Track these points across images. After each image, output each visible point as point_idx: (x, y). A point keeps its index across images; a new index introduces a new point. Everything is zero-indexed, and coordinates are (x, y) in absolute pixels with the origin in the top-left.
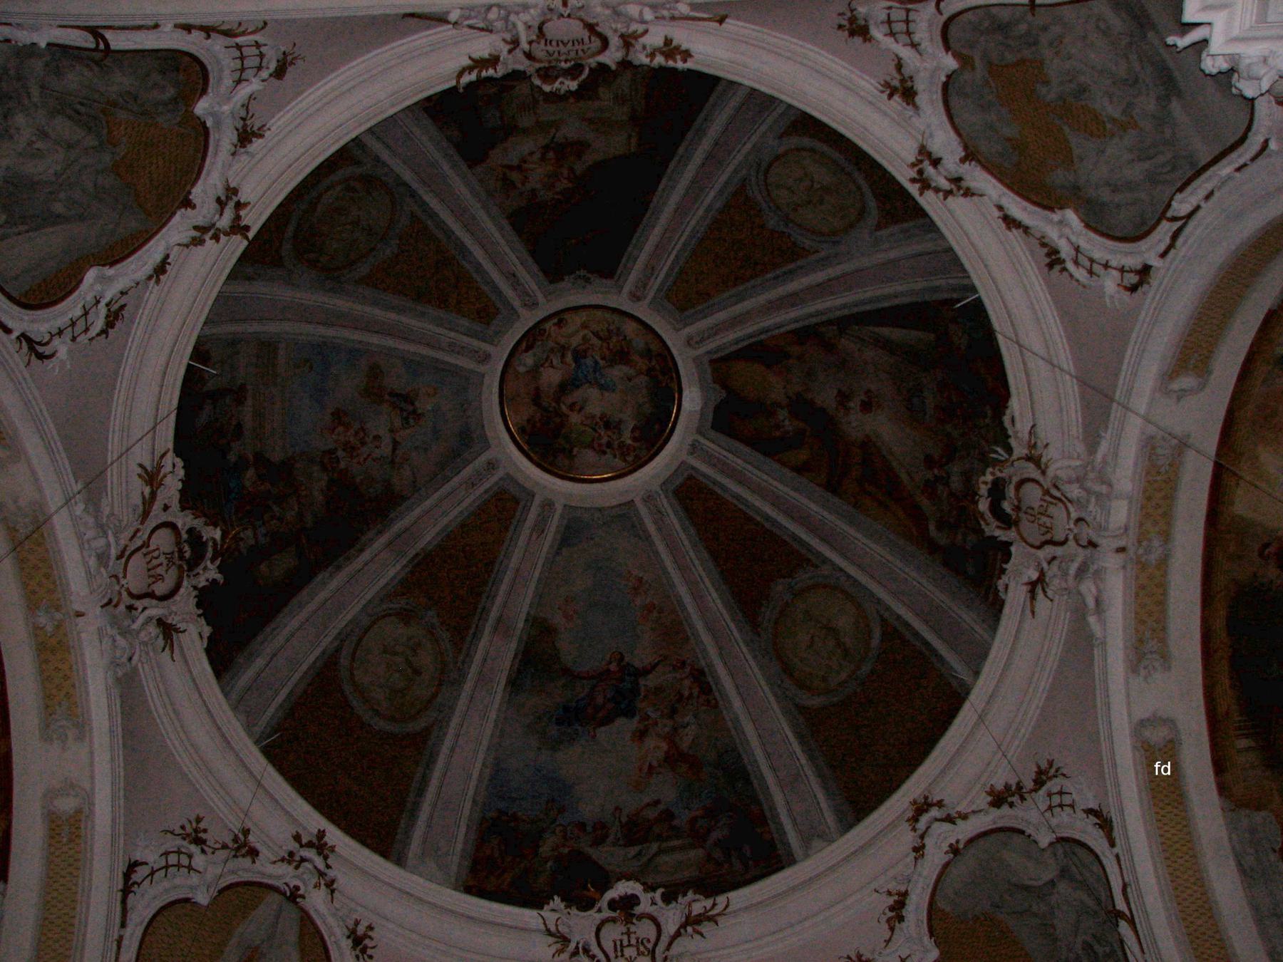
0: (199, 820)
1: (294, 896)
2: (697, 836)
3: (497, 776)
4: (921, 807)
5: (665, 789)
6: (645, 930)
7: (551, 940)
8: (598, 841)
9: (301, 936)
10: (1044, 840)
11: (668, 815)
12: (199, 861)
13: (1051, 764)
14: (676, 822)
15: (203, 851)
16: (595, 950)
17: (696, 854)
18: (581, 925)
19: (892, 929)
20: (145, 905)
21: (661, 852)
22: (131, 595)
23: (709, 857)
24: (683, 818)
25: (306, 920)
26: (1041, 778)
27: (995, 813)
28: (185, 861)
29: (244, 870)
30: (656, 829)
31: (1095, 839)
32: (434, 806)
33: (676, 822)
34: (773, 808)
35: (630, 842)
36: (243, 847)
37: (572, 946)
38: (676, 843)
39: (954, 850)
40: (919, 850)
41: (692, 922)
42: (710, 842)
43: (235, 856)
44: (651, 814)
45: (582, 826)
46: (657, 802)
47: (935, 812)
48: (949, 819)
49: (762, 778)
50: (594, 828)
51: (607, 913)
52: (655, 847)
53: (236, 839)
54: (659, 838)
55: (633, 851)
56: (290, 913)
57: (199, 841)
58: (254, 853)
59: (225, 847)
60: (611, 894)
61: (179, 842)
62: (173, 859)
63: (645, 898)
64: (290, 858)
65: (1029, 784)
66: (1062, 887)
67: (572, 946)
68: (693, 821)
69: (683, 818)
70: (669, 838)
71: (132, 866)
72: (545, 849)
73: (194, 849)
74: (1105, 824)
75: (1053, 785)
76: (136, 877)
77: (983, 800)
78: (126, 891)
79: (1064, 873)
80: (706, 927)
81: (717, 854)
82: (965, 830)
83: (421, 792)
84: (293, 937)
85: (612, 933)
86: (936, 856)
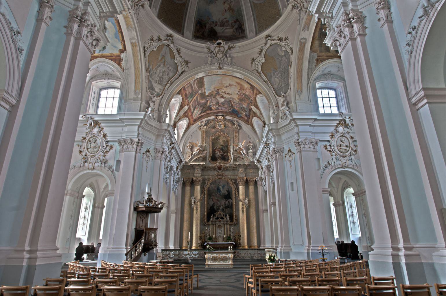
0: (152, 36)
1: (168, 45)
2: (233, 27)
3: (198, 10)
4: (268, 36)
5: (228, 15)
6: (222, 49)
7: (207, 50)
8: (216, 26)
9: (170, 52)
10: (283, 49)
11: (228, 21)
12: (153, 44)
13: (288, 37)
14: (229, 23)
15: (154, 42)
16: (214, 52)
17: (232, 30)
18: (213, 46)
19: (259, 55)
20: (147, 54)
21: (226, 29)
22: (136, 2)
23: (234, 31)
24: (230, 22)
25: (170, 49)
26: (286, 39)
27: (278, 41)
28: (151, 44)
29: (160, 43)
30: (225, 24)
31: (290, 52)
32: (188, 19)
33: (229, 23)
34: (245, 22)
35: (221, 26)
36: (159, 39)
37: (210, 51)
38: (228, 27)
39: (271, 45)
40: (266, 44)
41: (229, 48)
42: (234, 28)
43: (159, 41)
44: (225, 20)
45: (213, 22)
46: (226, 18)
47: (269, 38)
48: (271, 40)
49: (244, 16)
50: (215, 23)
51: (216, 45)
52: (225, 28)
53: (158, 38)
54: (226, 26)
55: (221, 28)
56: (168, 48)
57: (153, 40)
58: (161, 40)
59: (157, 39)
60: (217, 42)
61: (150, 41)
62: (150, 44)
63: (222, 43)
64: (167, 40)
65: (284, 39)
66: (284, 57)
67: (210, 51)
68: (232, 23)
69: (230, 22)
70: (227, 26)
71: (144, 47)
72: (207, 27)
73: (152, 42)
74: (292, 51)
75: (287, 41)
76: (145, 49)
77: (277, 38)
78: (145, 51)
79: (285, 55)
80: (232, 49)
81: (235, 31)
82: (273, 42)
83: (186, 16)
84: (169, 52)
85: (217, 49)
86: (268, 45)
